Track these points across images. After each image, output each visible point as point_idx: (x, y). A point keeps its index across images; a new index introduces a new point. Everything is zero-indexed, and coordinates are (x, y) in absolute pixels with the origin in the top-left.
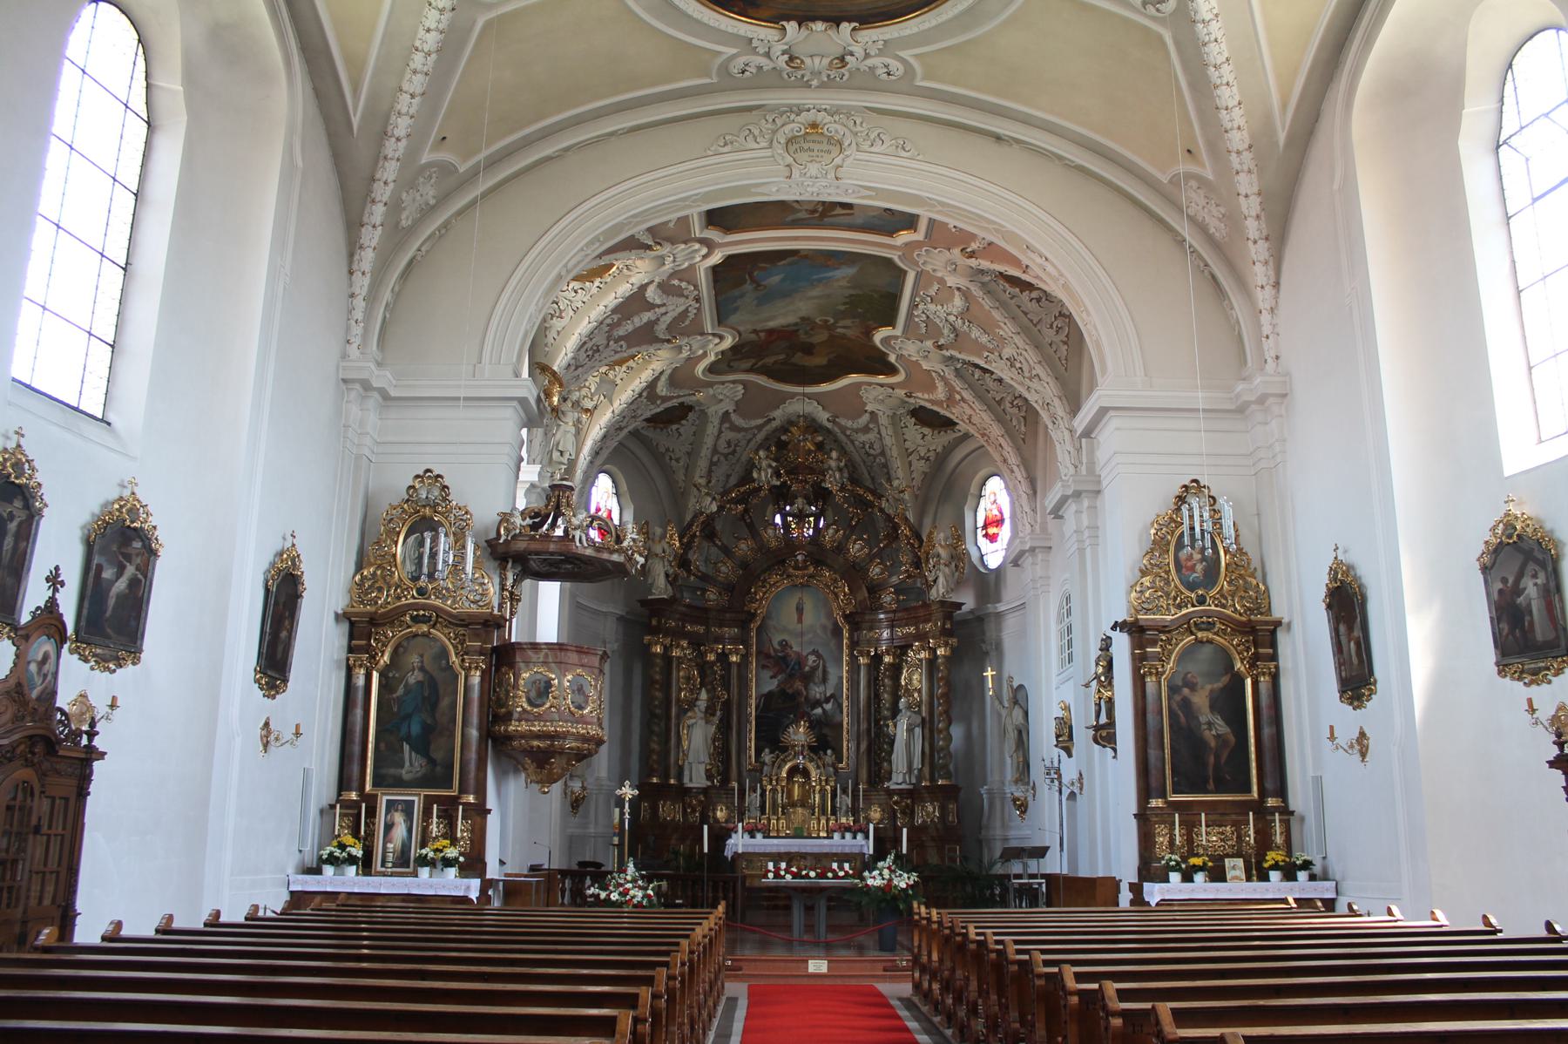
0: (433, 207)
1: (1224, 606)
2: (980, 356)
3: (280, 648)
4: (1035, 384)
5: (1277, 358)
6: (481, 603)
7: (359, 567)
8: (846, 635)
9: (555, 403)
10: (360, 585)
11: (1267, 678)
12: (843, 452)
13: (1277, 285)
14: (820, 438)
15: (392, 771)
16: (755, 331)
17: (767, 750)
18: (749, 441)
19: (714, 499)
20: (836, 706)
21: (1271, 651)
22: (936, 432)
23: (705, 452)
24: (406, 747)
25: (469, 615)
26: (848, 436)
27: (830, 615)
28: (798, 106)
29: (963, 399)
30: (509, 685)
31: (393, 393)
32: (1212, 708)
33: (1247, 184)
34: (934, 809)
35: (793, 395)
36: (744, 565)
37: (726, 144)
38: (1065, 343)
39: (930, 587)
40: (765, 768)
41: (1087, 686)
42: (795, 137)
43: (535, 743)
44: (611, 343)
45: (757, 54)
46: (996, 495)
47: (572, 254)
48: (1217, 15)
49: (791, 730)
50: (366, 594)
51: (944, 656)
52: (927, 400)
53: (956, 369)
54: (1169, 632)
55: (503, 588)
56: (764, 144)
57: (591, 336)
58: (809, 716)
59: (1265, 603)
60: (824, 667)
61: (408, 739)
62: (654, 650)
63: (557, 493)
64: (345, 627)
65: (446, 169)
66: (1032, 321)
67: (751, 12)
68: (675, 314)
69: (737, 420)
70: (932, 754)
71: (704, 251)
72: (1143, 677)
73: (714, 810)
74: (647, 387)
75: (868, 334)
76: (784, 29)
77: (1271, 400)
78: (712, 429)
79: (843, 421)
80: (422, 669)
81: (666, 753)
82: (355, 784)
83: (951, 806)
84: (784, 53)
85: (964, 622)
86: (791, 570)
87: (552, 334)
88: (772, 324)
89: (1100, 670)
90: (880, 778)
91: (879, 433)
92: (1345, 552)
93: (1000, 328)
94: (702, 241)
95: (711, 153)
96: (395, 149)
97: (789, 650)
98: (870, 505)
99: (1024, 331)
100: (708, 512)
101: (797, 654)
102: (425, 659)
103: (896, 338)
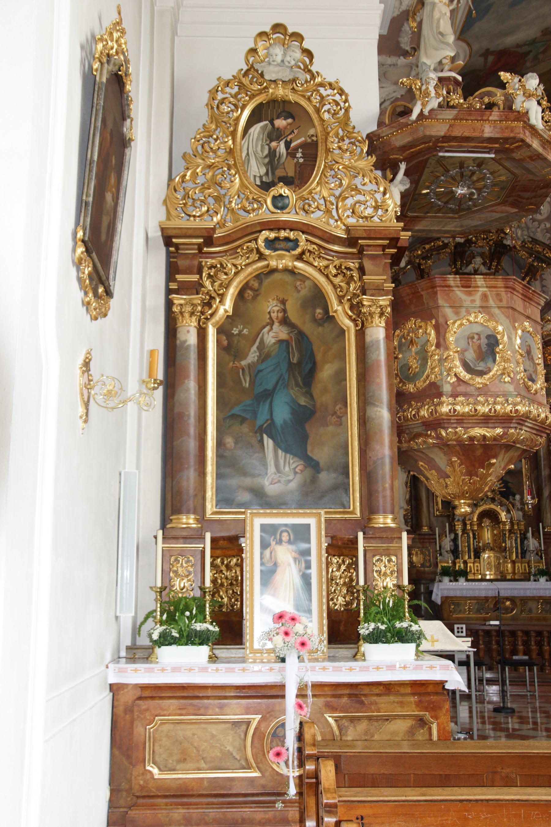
80: (285, 321)
102: (289, 306)
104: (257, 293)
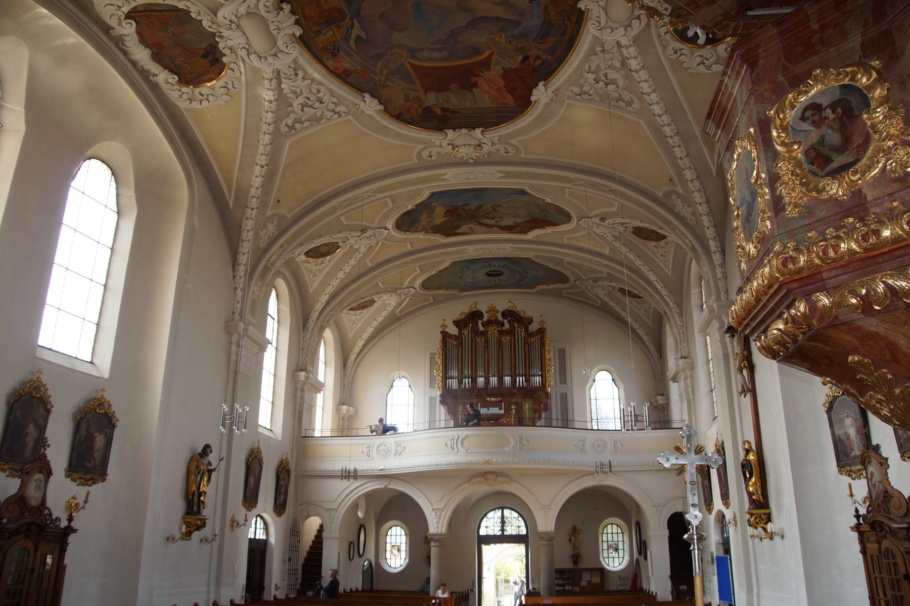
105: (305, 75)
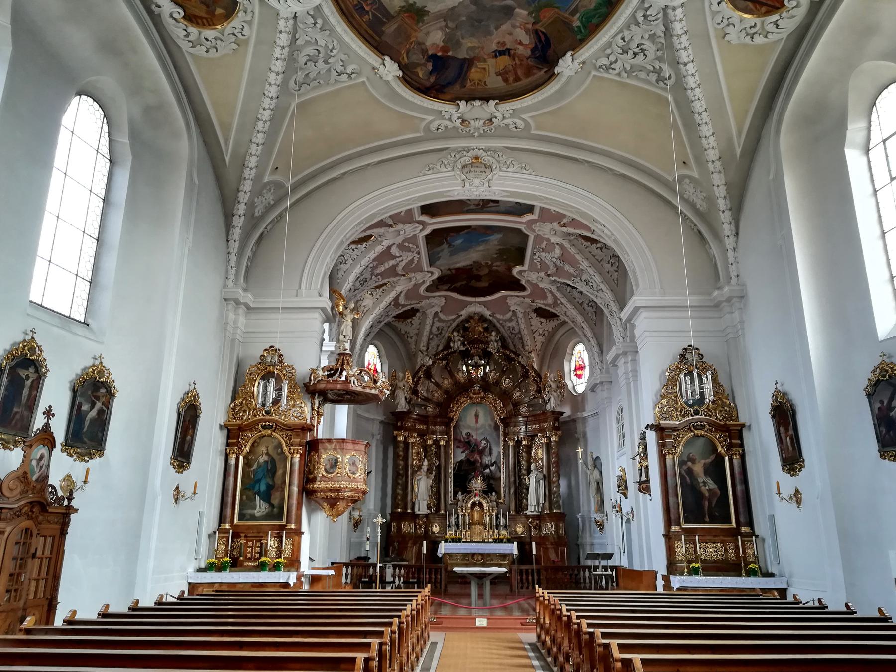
0: (272, 205)
1: (710, 416)
2: (570, 280)
3: (186, 446)
4: (600, 294)
5: (738, 276)
6: (300, 418)
7: (234, 399)
8: (501, 429)
9: (341, 310)
10: (234, 409)
11: (738, 457)
12: (498, 331)
13: (737, 234)
14: (486, 325)
15: (250, 511)
16: (450, 269)
17: (460, 493)
18: (449, 327)
19: (430, 358)
20: (497, 468)
21: (739, 441)
22: (548, 320)
23: (426, 333)
24: (258, 498)
25: (294, 424)
26: (501, 324)
27: (493, 419)
28: (468, 147)
29: (562, 303)
30: (315, 462)
31: (252, 305)
32: (706, 473)
33: (718, 179)
34: (552, 526)
35: (471, 303)
36: (446, 392)
37: (429, 169)
38: (616, 271)
39: (546, 403)
40: (459, 503)
41: (633, 459)
42: (467, 165)
43: (329, 494)
44: (373, 277)
45: (445, 119)
46: (581, 353)
47: (349, 229)
48: (699, 85)
49: (473, 482)
50: (237, 414)
51: (555, 441)
52: (543, 304)
53: (557, 287)
54: (678, 430)
55: (313, 409)
56: (449, 169)
57: (362, 274)
58: (482, 473)
59: (734, 414)
60: (490, 447)
61: (259, 493)
62: (399, 439)
63: (342, 357)
64: (226, 431)
65: (279, 185)
66: (598, 260)
67: (440, 96)
68: (407, 261)
69: (441, 315)
70: (550, 495)
71: (421, 227)
72: (664, 456)
73: (432, 526)
74: (393, 300)
75: (510, 270)
76: (458, 104)
77: (734, 300)
78: (429, 321)
79: (498, 316)
80: (267, 454)
81: (405, 495)
82: (228, 519)
83: (561, 525)
84: (459, 118)
85: (565, 422)
86: (472, 395)
87: (341, 273)
88: (458, 265)
89: (641, 450)
90: (522, 508)
91: (517, 322)
92: (782, 385)
93: (580, 264)
94: (420, 222)
95: (422, 174)
96: (249, 174)
97: (471, 438)
98: (514, 360)
99: (592, 265)
100: (427, 365)
101: (476, 440)
102: (269, 448)
103: (525, 271)
104: (259, 443)
105: (323, 25)
